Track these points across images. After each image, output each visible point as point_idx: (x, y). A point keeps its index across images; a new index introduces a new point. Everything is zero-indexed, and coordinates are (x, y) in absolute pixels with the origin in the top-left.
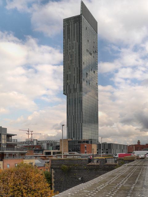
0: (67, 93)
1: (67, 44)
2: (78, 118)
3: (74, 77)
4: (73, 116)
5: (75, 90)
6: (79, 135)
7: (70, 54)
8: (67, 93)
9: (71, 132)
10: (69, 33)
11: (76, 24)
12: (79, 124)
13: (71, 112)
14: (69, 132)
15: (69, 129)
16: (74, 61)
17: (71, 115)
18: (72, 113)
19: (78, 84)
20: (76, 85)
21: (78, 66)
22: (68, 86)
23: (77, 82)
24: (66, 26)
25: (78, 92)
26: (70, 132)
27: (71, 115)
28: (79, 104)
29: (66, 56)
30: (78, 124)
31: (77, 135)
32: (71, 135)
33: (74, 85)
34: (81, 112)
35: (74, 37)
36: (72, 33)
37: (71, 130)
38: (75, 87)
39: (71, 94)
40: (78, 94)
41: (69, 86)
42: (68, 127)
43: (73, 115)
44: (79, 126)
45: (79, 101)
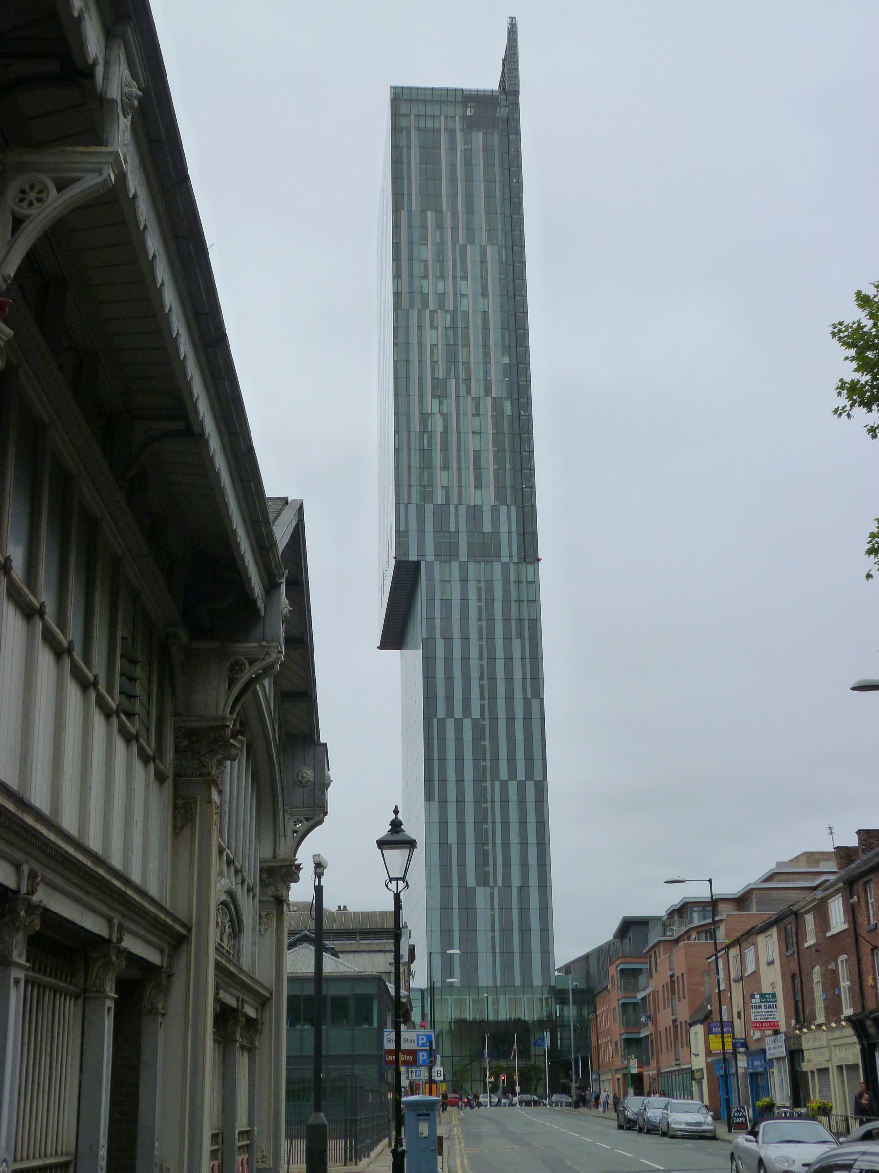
1: (416, 239)
2: (511, 739)
4: (476, 724)
5: (485, 550)
6: (524, 865)
7: (441, 305)
9: (461, 843)
11: (478, 138)
12: (521, 786)
13: (458, 693)
15: (443, 822)
16: (475, 353)
17: (458, 713)
18: (467, 699)
19: (503, 509)
20: (495, 510)
22: (429, 508)
24: (414, 135)
25: (505, 558)
26: (452, 838)
27: (459, 714)
28: (516, 644)
30: (513, 786)
31: (507, 865)
32: (462, 865)
33: (475, 513)
34: (535, 703)
35: (470, 210)
36: (453, 180)
37: (461, 823)
38: (487, 528)
39: (455, 566)
40: (506, 581)
41: (441, 513)
42: (435, 805)
43: (476, 714)
44: (522, 801)
45: (520, 621)
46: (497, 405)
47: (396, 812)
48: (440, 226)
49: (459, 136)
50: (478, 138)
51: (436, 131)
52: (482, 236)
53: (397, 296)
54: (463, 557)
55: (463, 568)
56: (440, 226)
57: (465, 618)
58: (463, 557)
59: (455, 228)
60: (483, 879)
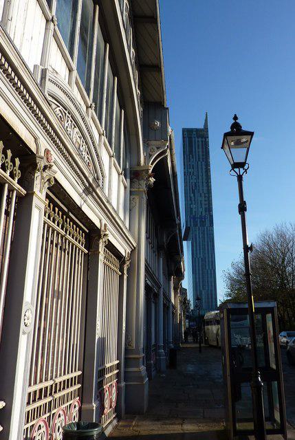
14: (196, 281)
15: (196, 278)
47: (235, 118)
48: (193, 158)
52: (201, 160)
53: (185, 172)
56: (193, 158)
60: (203, 289)
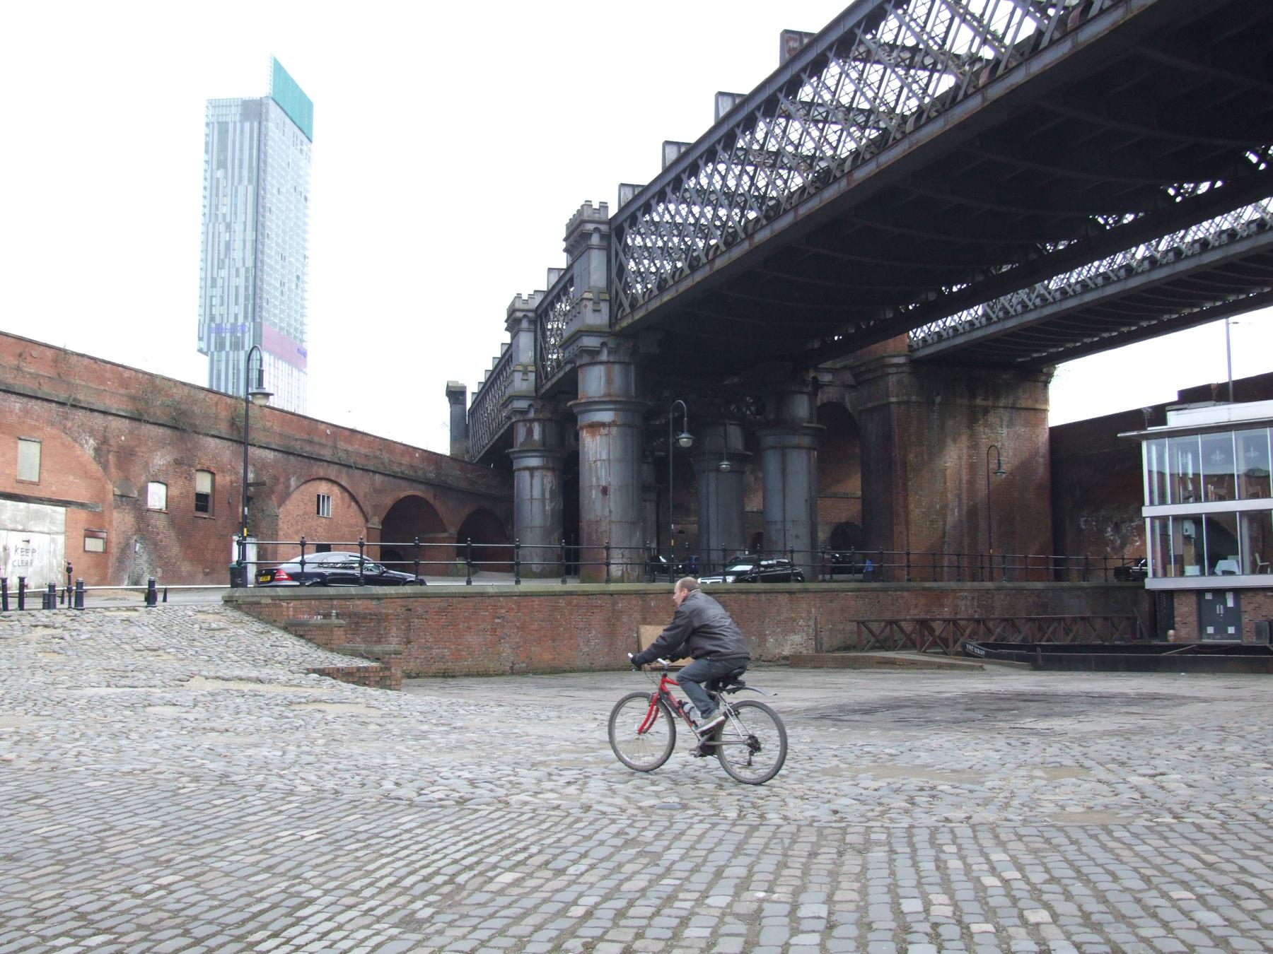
0: (209, 348)
3: (237, 299)
8: (209, 348)
10: (223, 148)
11: (247, 125)
21: (250, 263)
22: (213, 325)
23: (246, 318)
29: (211, 226)
35: (241, 166)
39: (224, 353)
46: (247, 270)
49: (238, 125)
50: (247, 125)
51: (227, 123)
52: (245, 181)
54: (228, 349)
55: (227, 354)
57: (227, 379)
58: (228, 349)
59: (233, 177)
